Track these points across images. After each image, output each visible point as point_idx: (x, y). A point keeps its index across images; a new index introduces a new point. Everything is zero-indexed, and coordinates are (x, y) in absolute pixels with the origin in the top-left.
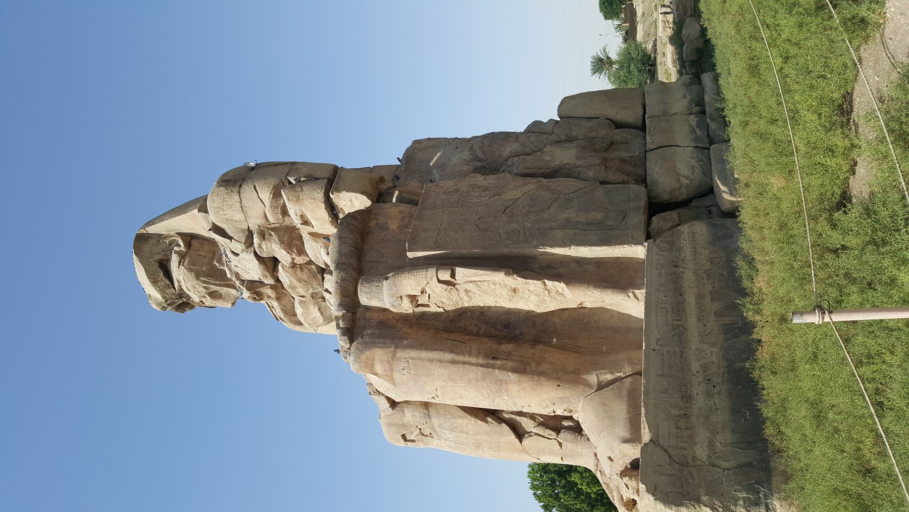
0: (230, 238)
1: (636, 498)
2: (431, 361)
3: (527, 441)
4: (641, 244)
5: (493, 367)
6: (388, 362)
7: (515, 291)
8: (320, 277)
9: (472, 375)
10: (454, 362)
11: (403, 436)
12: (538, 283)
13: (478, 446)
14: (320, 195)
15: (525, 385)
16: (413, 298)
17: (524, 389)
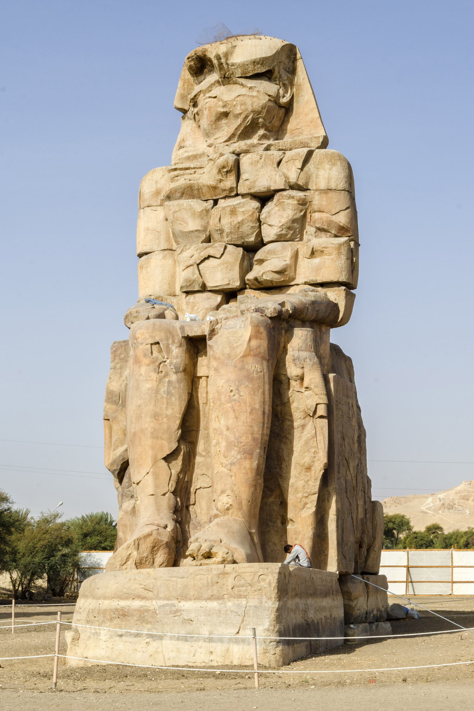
0: (302, 169)
1: (218, 558)
2: (264, 393)
3: (163, 463)
4: (338, 569)
5: (261, 448)
6: (260, 353)
7: (309, 469)
8: (239, 243)
9: (256, 429)
10: (264, 413)
11: (158, 343)
12: (316, 489)
13: (156, 416)
14: (343, 278)
15: (250, 475)
16: (302, 379)
17: (247, 473)
